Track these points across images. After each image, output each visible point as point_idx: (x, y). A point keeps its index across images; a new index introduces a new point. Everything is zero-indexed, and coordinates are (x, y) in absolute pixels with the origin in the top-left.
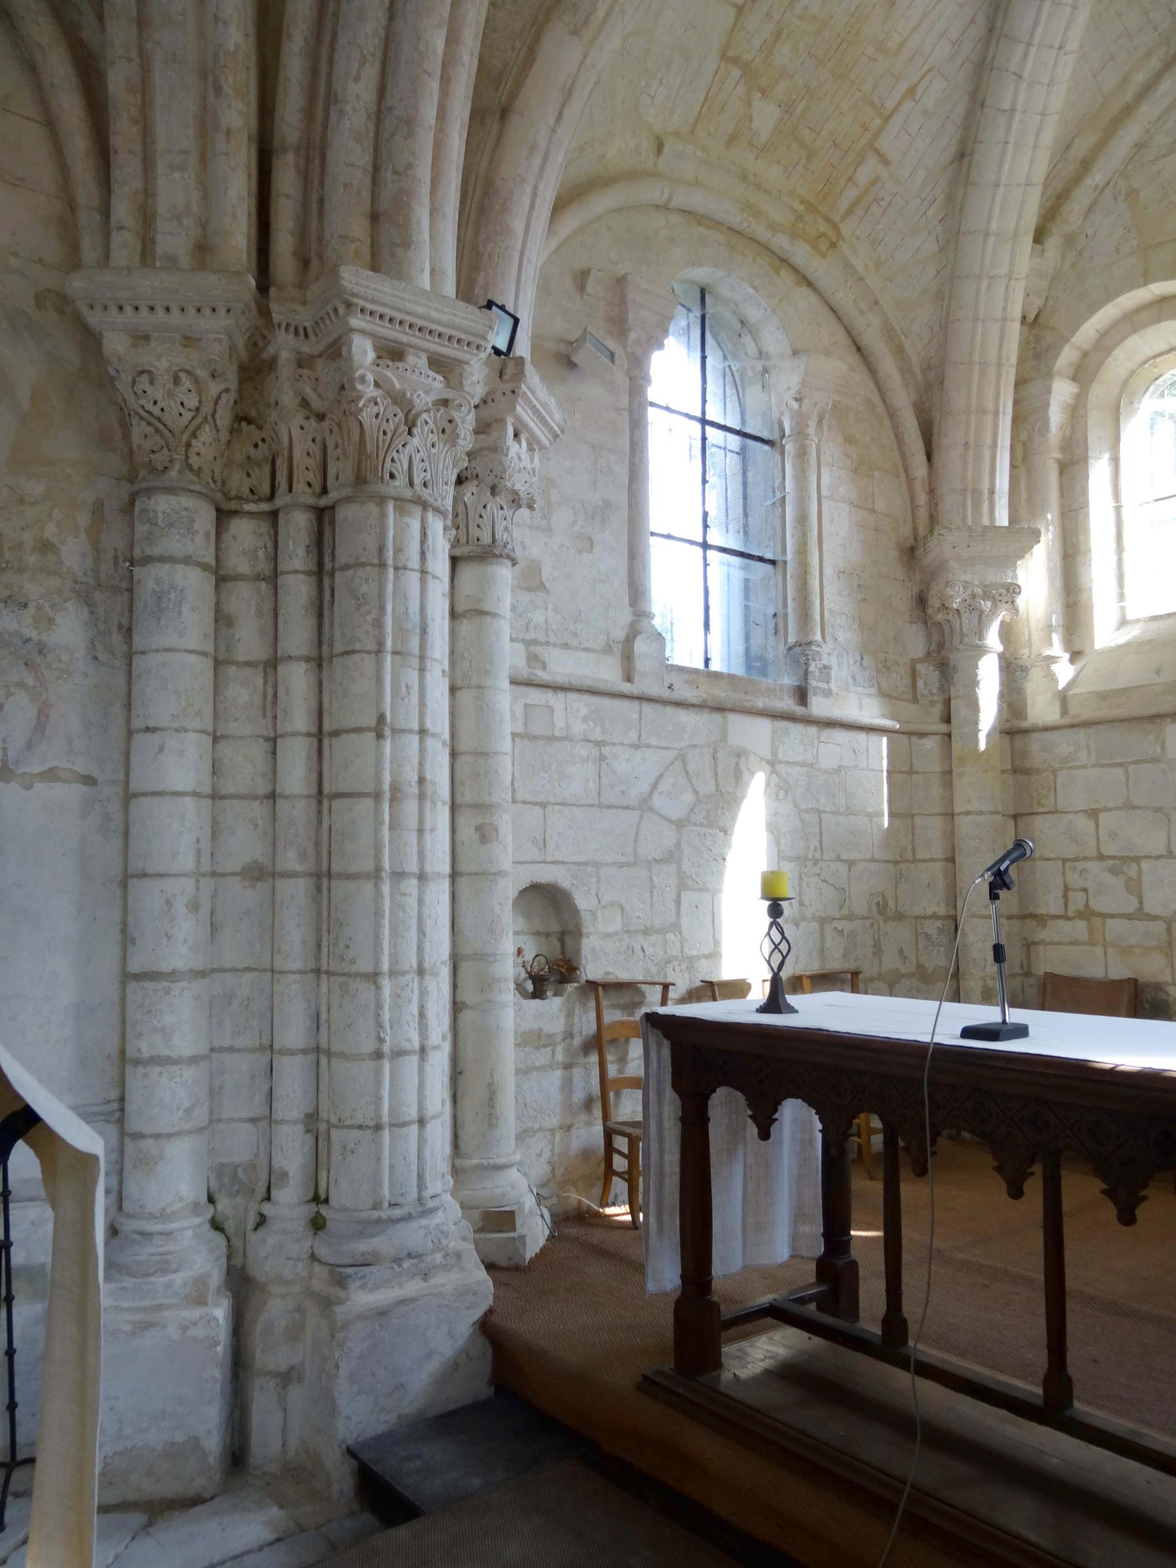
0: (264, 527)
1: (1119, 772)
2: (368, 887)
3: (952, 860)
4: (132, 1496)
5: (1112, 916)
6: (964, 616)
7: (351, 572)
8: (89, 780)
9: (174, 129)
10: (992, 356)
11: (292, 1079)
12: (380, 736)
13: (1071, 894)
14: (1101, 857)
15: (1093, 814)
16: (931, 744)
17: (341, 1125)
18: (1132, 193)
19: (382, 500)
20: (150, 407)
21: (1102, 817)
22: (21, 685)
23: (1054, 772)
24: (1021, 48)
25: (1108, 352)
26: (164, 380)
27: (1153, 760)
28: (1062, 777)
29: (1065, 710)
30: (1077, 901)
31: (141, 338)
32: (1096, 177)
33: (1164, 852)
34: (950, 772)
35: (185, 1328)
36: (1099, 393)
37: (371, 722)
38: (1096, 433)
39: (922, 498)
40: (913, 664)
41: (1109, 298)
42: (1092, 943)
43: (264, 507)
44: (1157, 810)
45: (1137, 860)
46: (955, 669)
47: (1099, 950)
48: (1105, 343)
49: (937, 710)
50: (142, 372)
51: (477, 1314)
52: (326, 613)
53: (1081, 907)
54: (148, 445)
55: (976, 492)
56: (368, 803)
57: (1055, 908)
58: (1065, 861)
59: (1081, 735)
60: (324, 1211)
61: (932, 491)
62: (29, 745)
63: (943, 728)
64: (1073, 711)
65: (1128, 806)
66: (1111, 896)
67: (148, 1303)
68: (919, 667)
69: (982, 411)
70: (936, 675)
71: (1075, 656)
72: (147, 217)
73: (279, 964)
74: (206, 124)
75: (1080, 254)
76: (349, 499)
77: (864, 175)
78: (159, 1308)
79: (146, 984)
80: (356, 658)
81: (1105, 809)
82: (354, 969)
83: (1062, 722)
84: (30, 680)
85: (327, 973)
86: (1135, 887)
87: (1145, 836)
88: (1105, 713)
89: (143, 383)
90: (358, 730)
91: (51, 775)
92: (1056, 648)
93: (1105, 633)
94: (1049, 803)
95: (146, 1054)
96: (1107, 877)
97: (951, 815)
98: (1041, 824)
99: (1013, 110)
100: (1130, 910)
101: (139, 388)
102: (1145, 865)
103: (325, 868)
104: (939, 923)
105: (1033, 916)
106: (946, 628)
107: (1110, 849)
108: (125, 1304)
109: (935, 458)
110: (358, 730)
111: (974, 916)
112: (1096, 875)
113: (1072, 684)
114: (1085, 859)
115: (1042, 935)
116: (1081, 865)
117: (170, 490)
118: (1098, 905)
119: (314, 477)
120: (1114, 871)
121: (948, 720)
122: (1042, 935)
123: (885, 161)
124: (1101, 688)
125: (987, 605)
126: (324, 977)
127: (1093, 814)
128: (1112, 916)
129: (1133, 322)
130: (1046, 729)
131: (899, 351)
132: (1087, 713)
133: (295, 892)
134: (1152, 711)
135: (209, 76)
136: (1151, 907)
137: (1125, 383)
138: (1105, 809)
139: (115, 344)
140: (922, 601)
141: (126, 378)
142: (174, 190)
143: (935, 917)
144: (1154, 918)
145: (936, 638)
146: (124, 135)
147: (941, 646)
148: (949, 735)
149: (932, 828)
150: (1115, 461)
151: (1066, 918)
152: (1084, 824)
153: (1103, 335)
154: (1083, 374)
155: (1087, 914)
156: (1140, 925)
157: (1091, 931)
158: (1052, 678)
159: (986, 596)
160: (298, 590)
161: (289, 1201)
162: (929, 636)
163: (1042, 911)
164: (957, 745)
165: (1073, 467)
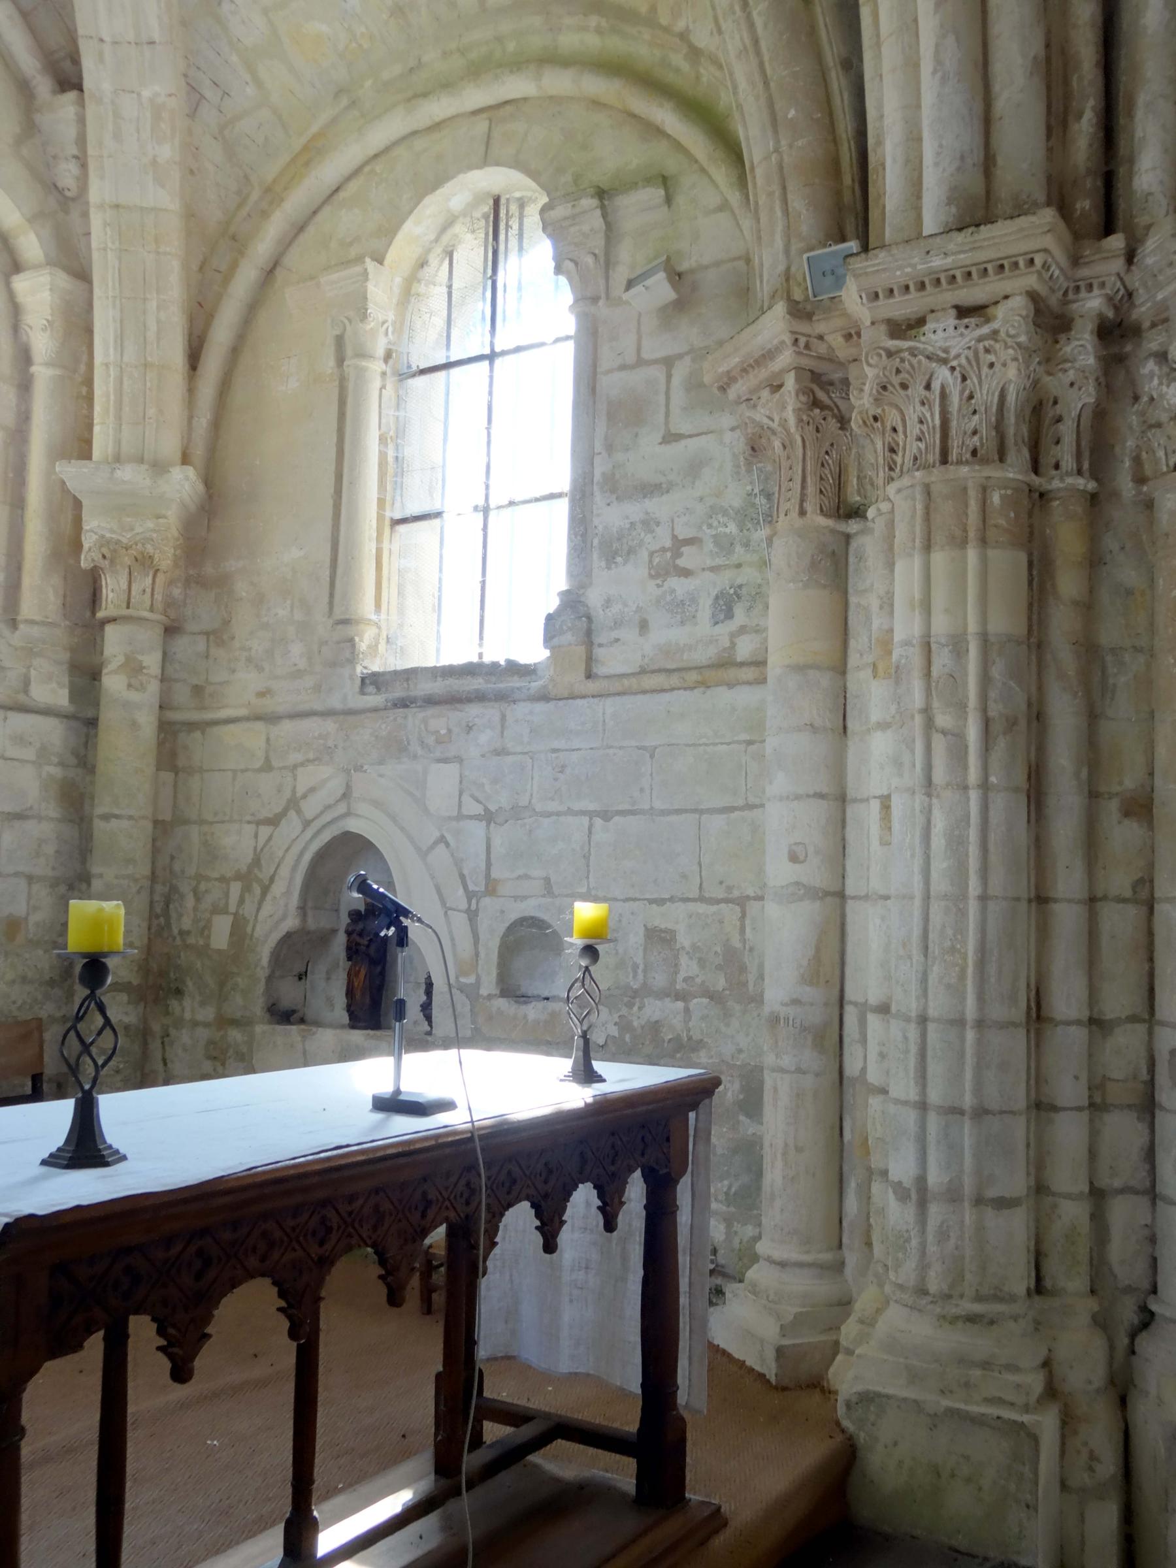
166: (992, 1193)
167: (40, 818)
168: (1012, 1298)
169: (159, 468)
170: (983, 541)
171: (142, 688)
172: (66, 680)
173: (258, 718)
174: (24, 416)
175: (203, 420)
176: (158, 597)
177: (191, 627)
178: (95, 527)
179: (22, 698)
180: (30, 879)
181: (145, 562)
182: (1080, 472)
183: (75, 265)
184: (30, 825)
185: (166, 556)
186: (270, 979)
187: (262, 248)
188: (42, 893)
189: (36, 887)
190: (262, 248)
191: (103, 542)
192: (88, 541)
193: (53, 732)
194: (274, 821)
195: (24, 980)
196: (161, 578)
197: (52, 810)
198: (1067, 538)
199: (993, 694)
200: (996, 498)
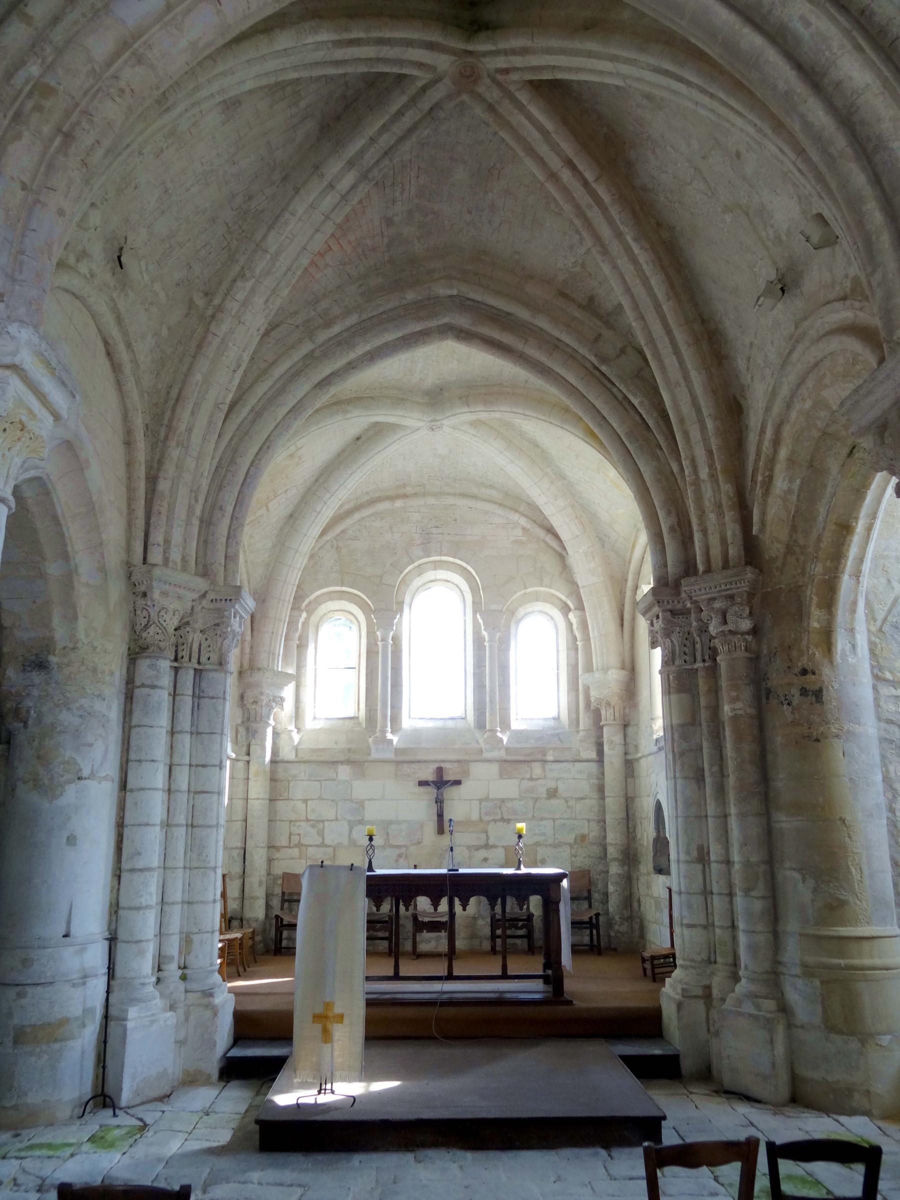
0: (173, 673)
1: (318, 784)
2: (215, 830)
3: (246, 821)
4: (145, 1099)
5: (311, 846)
6: (263, 709)
7: (214, 701)
8: (113, 781)
9: (181, 512)
10: (287, 599)
11: (176, 916)
12: (221, 769)
13: (292, 837)
14: (308, 820)
15: (305, 801)
16: (241, 765)
17: (200, 932)
18: (338, 549)
19: (226, 672)
20: (162, 622)
21: (309, 802)
22: (101, 736)
23: (289, 782)
24: (329, 495)
25: (320, 604)
26: (170, 613)
27: (334, 780)
28: (292, 784)
29: (296, 756)
30: (295, 839)
31: (165, 594)
32: (327, 537)
33: (334, 818)
34: (248, 779)
35: (166, 1021)
36: (314, 619)
37: (217, 762)
38: (311, 636)
39: (247, 650)
40: (237, 725)
41: (327, 586)
42: (300, 858)
43: (176, 664)
44: (333, 801)
45: (323, 821)
46: (256, 731)
47: (303, 861)
48: (318, 602)
49: (244, 749)
50: (163, 608)
51: (232, 1010)
52: (195, 714)
53: (297, 842)
54: (158, 637)
55: (274, 654)
56: (215, 797)
57: (284, 842)
58: (291, 821)
59: (302, 767)
60: (186, 971)
61: (252, 648)
62: (102, 763)
63: (247, 758)
64: (299, 756)
65: (320, 798)
66: (310, 836)
67: (150, 1013)
68: (239, 728)
69: (280, 620)
70: (244, 733)
71: (299, 730)
72: (167, 542)
73: (169, 864)
74: (191, 510)
75: (316, 563)
76: (215, 670)
77: (259, 513)
78: (153, 1015)
79: (146, 873)
80: (214, 736)
81: (311, 799)
82: (210, 865)
83: (296, 760)
84: (104, 734)
85: (190, 869)
86: (321, 833)
87: (328, 812)
88: (314, 758)
89: (162, 613)
90: (214, 766)
91: (105, 778)
92: (292, 727)
93: (310, 724)
94: (285, 795)
95: (144, 904)
96: (309, 829)
97: (247, 799)
98: (280, 805)
99: (319, 513)
100: (318, 843)
101: (161, 614)
102: (326, 824)
103: (190, 823)
104: (238, 851)
105: (273, 847)
106: (253, 713)
107: (312, 816)
108: (142, 1015)
109: (255, 633)
110: (214, 766)
111: (258, 847)
112: (305, 827)
113: (299, 743)
114: (300, 821)
115: (277, 855)
116: (298, 824)
117: (165, 659)
118: (303, 841)
119: (197, 656)
120: (313, 826)
121: (248, 754)
122: (277, 855)
123: (268, 510)
124: (313, 747)
125: (274, 704)
126: (188, 870)
127: (305, 801)
128: (311, 846)
129: (331, 596)
130: (287, 762)
131: (249, 583)
132: (307, 758)
133: (180, 833)
134: (335, 760)
135: (194, 492)
136: (328, 841)
137: (322, 618)
138: (311, 799)
139: (156, 594)
140: (242, 697)
141: (157, 609)
142: (177, 536)
143: (237, 848)
144: (329, 846)
145: (246, 715)
146: (161, 505)
147: (248, 719)
148: (248, 762)
149: (239, 804)
150: (316, 648)
151: (290, 847)
152: (300, 805)
153: (318, 597)
154: (310, 613)
155: (299, 845)
156: (322, 849)
157: (300, 852)
158: (291, 738)
159: (274, 701)
160: (186, 703)
161: (172, 969)
162: (244, 714)
163: (278, 844)
164: (253, 768)
165: (302, 647)
166: (684, 922)
167: (591, 799)
168: (693, 960)
169: (605, 670)
170: (669, 692)
171: (613, 749)
172: (595, 748)
173: (644, 756)
174: (577, 659)
175: (627, 646)
176: (617, 715)
177: (632, 723)
178: (594, 694)
179: (578, 758)
180: (589, 821)
181: (608, 704)
182: (704, 661)
183: (581, 607)
184: (587, 801)
185: (615, 701)
186: (654, 857)
187: (630, 583)
188: (595, 826)
189: (591, 824)
190: (630, 583)
191: (596, 699)
192: (592, 699)
193: (593, 767)
194: (649, 796)
195: (589, 857)
196: (617, 709)
197: (595, 795)
198: (702, 684)
199: (675, 745)
200: (671, 678)
